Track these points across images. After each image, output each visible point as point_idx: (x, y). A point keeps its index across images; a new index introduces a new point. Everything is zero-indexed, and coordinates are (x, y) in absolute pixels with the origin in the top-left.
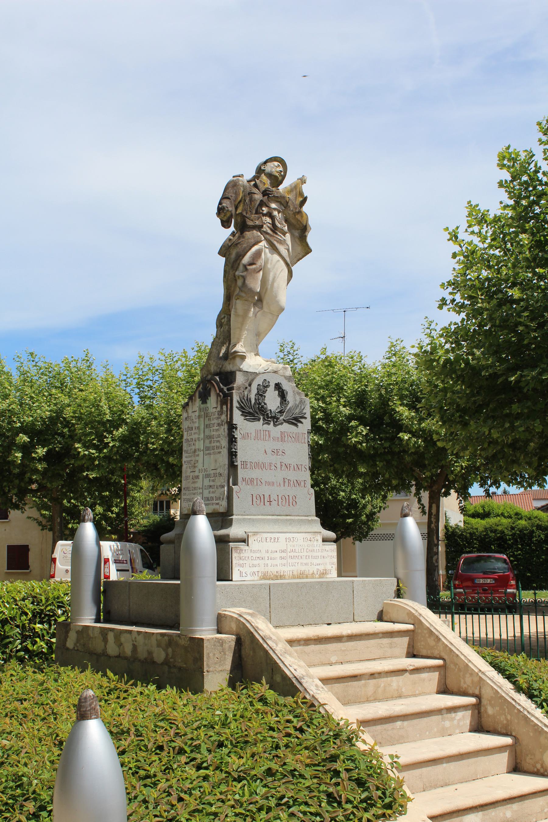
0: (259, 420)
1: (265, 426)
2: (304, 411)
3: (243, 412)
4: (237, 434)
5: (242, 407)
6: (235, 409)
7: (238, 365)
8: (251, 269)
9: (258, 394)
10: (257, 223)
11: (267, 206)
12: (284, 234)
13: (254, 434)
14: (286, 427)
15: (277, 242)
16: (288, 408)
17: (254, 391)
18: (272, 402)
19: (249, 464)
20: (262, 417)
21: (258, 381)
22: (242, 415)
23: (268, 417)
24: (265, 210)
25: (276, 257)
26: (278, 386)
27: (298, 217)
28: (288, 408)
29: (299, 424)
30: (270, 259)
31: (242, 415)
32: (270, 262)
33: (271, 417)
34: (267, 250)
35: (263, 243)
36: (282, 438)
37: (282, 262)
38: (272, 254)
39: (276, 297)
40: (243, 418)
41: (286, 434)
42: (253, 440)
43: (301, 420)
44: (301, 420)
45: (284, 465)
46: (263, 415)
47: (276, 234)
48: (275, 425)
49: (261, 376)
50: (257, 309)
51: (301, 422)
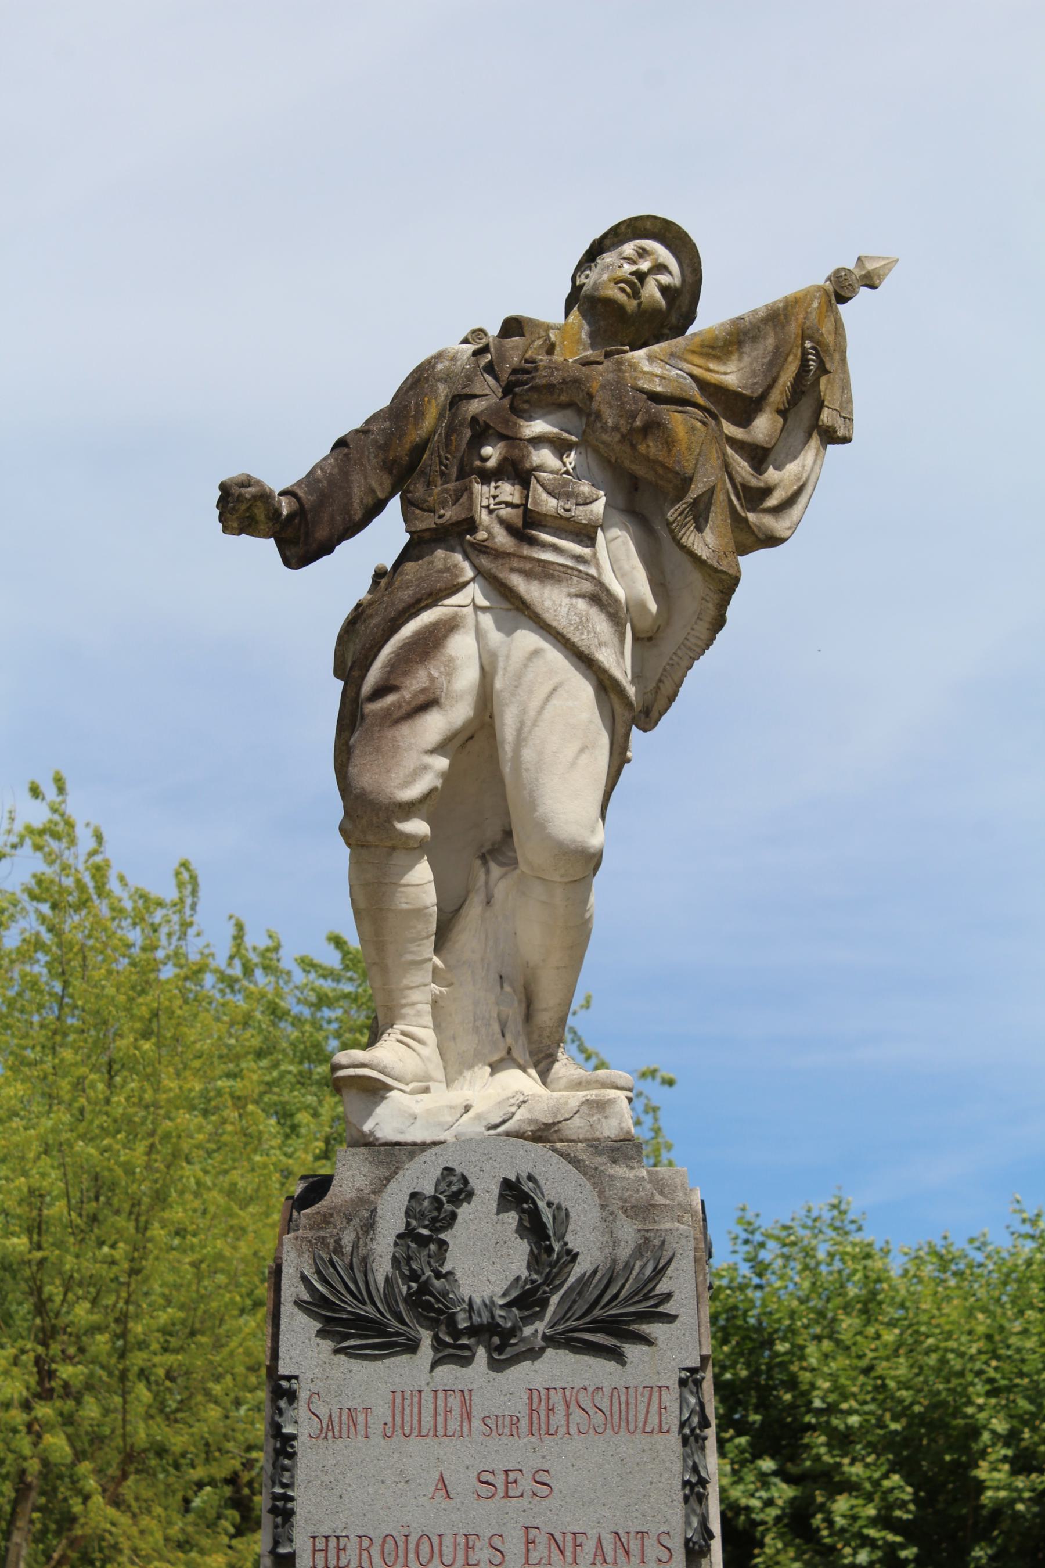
0: (412, 1347)
1: (447, 1373)
2: (663, 1287)
3: (327, 1320)
4: (300, 1423)
5: (322, 1301)
6: (288, 1308)
7: (353, 1119)
8: (375, 714)
9: (408, 1235)
10: (450, 514)
11: (503, 437)
12: (586, 534)
13: (382, 1412)
14: (558, 1368)
15: (528, 575)
16: (572, 1279)
17: (391, 1220)
18: (484, 1261)
19: (352, 1545)
20: (426, 1337)
21: (421, 1177)
22: (322, 1333)
23: (456, 1334)
24: (492, 453)
25: (528, 639)
26: (515, 1195)
27: (651, 447)
28: (572, 1279)
29: (632, 1351)
30: (502, 652)
31: (322, 1333)
32: (501, 664)
33: (473, 1331)
34: (487, 621)
35: (474, 593)
36: (538, 1415)
37: (555, 657)
38: (509, 632)
39: (532, 805)
40: (328, 1345)
41: (556, 1398)
42: (377, 1439)
43: (646, 1328)
44: (646, 1328)
45: (542, 1539)
46: (432, 1324)
47: (533, 542)
48: (497, 1365)
49: (429, 1155)
50: (496, 870)
51: (646, 1340)
